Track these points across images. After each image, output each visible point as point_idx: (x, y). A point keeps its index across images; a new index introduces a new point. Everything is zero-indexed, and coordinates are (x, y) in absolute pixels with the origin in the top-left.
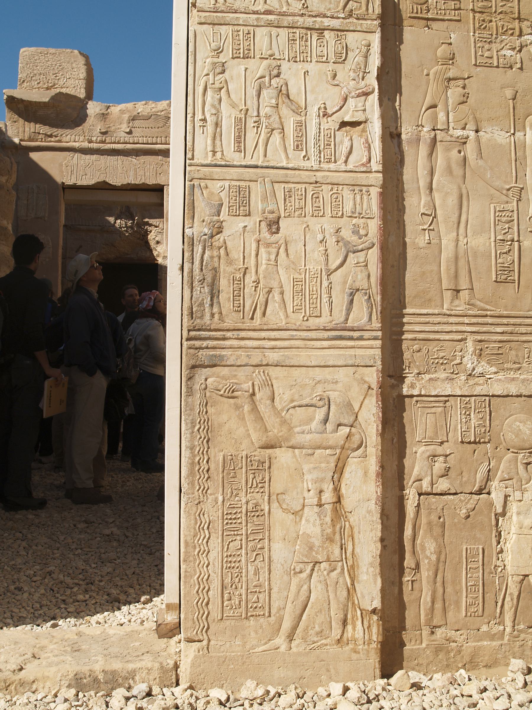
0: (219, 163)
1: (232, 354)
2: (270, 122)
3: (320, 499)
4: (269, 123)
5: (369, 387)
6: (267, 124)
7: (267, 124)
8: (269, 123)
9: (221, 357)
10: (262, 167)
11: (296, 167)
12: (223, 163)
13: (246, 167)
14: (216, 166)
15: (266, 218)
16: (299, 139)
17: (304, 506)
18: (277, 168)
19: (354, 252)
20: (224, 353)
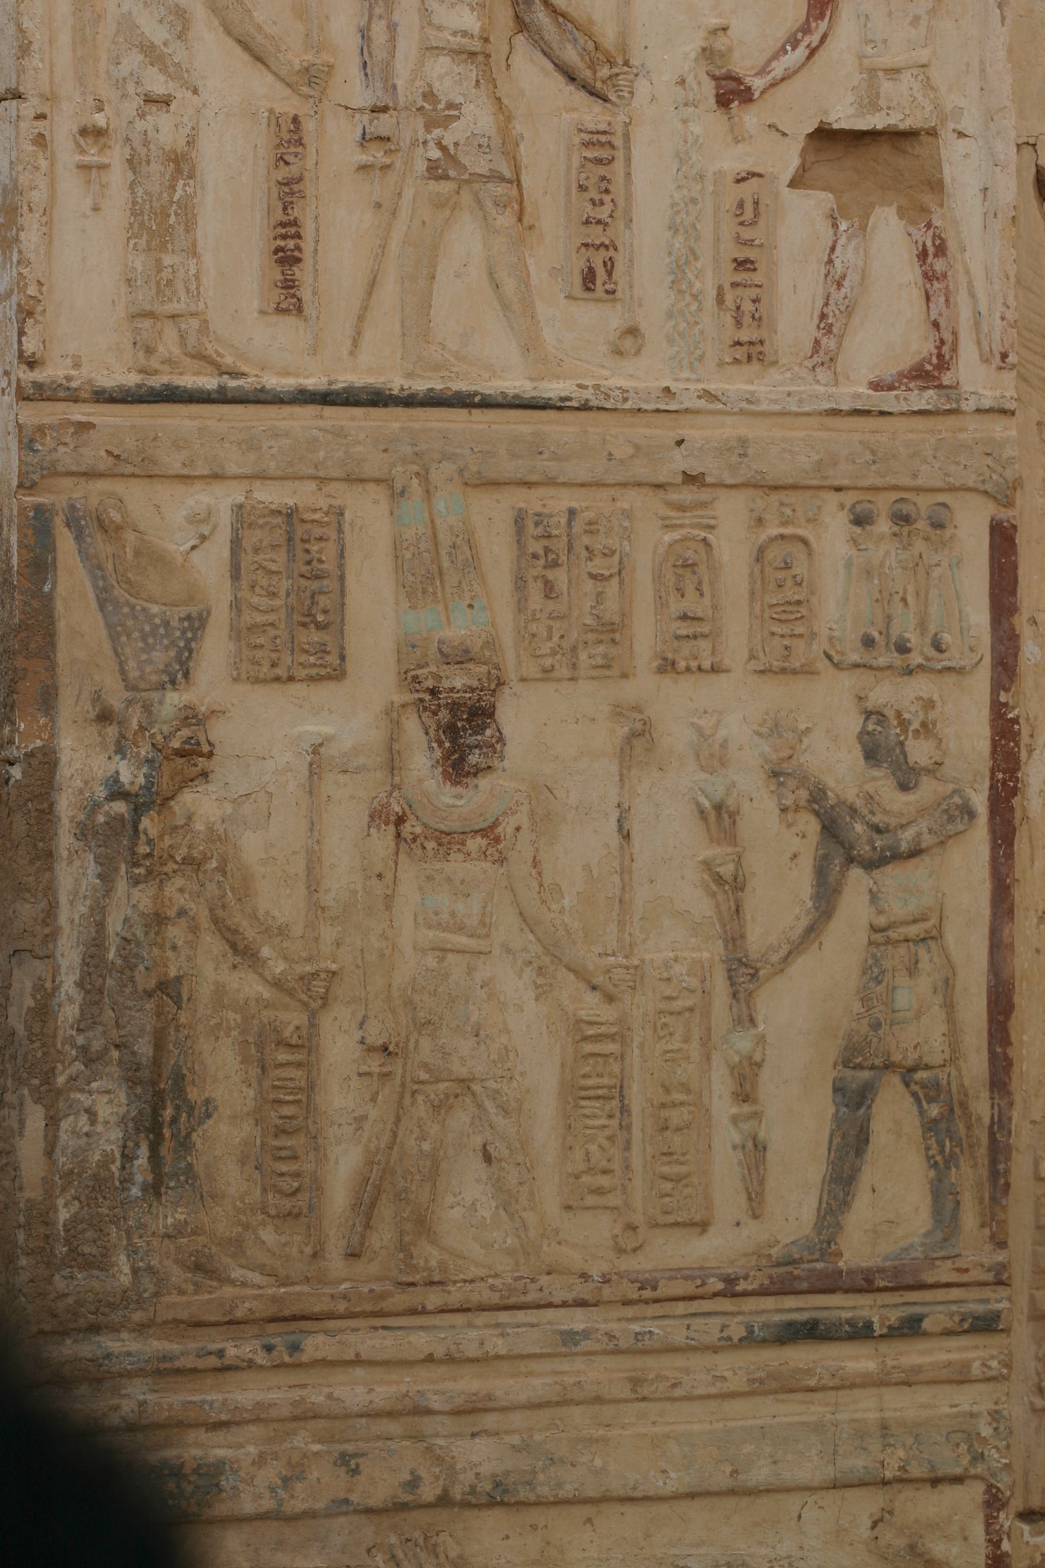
0: (188, 381)
1: (262, 1456)
2: (448, 141)
4: (443, 149)
6: (435, 154)
7: (435, 154)
8: (443, 149)
10: (410, 401)
11: (588, 394)
12: (209, 383)
13: (325, 398)
14: (171, 396)
15: (433, 692)
16: (596, 235)
18: (487, 403)
19: (870, 865)
20: (221, 1453)
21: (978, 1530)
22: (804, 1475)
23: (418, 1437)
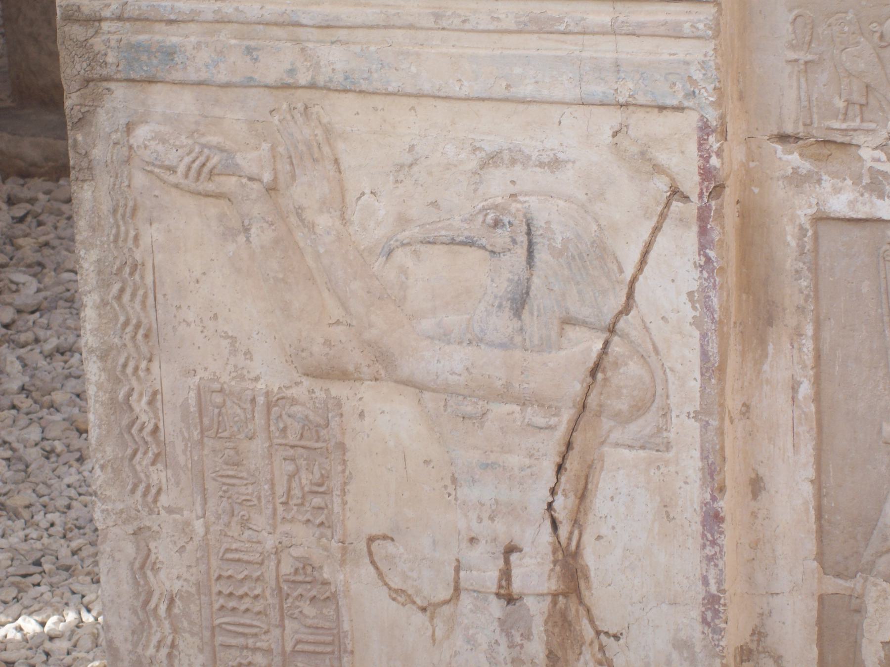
1: (199, 43)
3: (506, 574)
5: (675, 193)
9: (170, 53)
17: (457, 589)
20: (175, 40)
21: (692, 147)
22: (558, 93)
23: (297, 41)
